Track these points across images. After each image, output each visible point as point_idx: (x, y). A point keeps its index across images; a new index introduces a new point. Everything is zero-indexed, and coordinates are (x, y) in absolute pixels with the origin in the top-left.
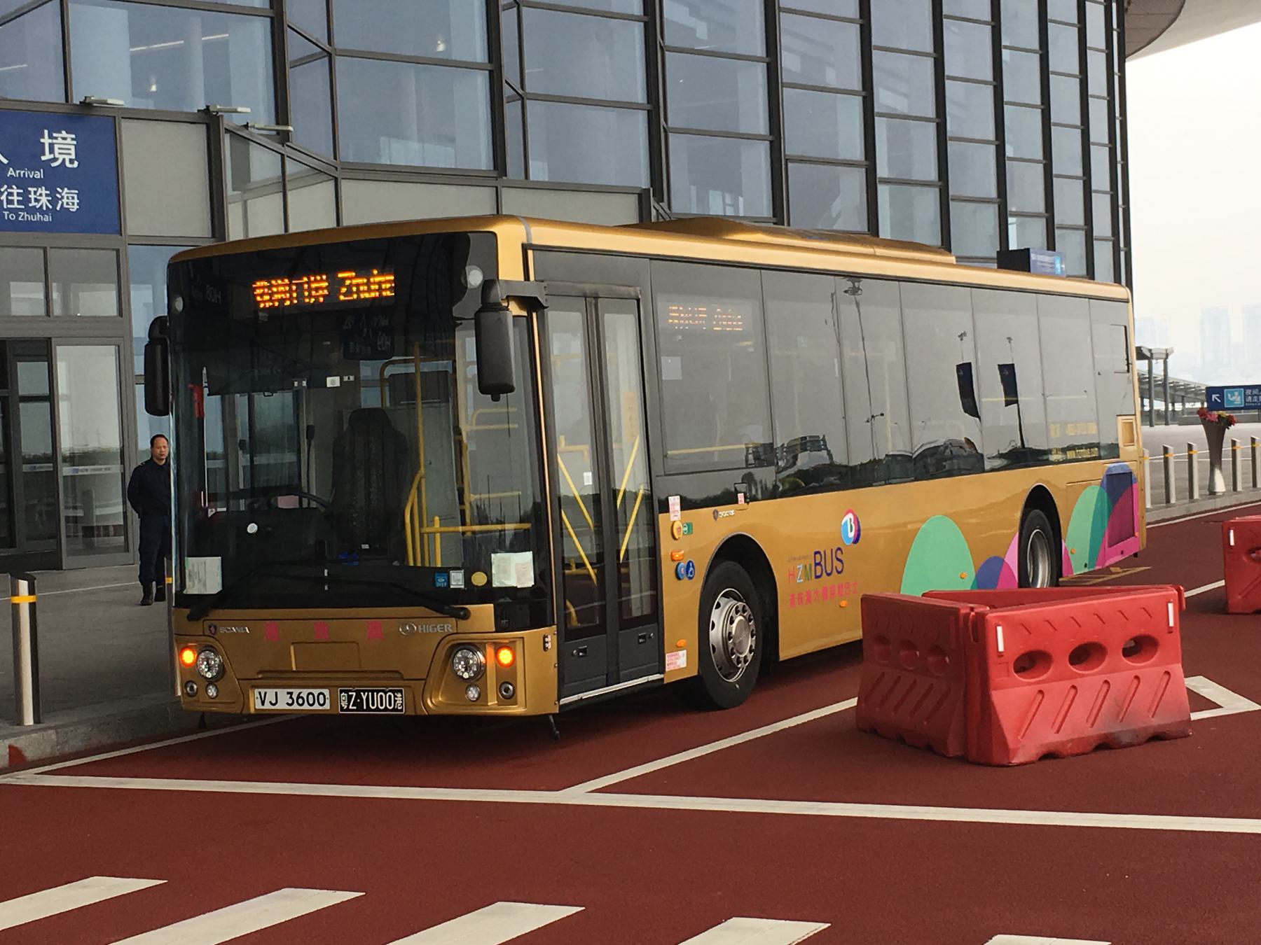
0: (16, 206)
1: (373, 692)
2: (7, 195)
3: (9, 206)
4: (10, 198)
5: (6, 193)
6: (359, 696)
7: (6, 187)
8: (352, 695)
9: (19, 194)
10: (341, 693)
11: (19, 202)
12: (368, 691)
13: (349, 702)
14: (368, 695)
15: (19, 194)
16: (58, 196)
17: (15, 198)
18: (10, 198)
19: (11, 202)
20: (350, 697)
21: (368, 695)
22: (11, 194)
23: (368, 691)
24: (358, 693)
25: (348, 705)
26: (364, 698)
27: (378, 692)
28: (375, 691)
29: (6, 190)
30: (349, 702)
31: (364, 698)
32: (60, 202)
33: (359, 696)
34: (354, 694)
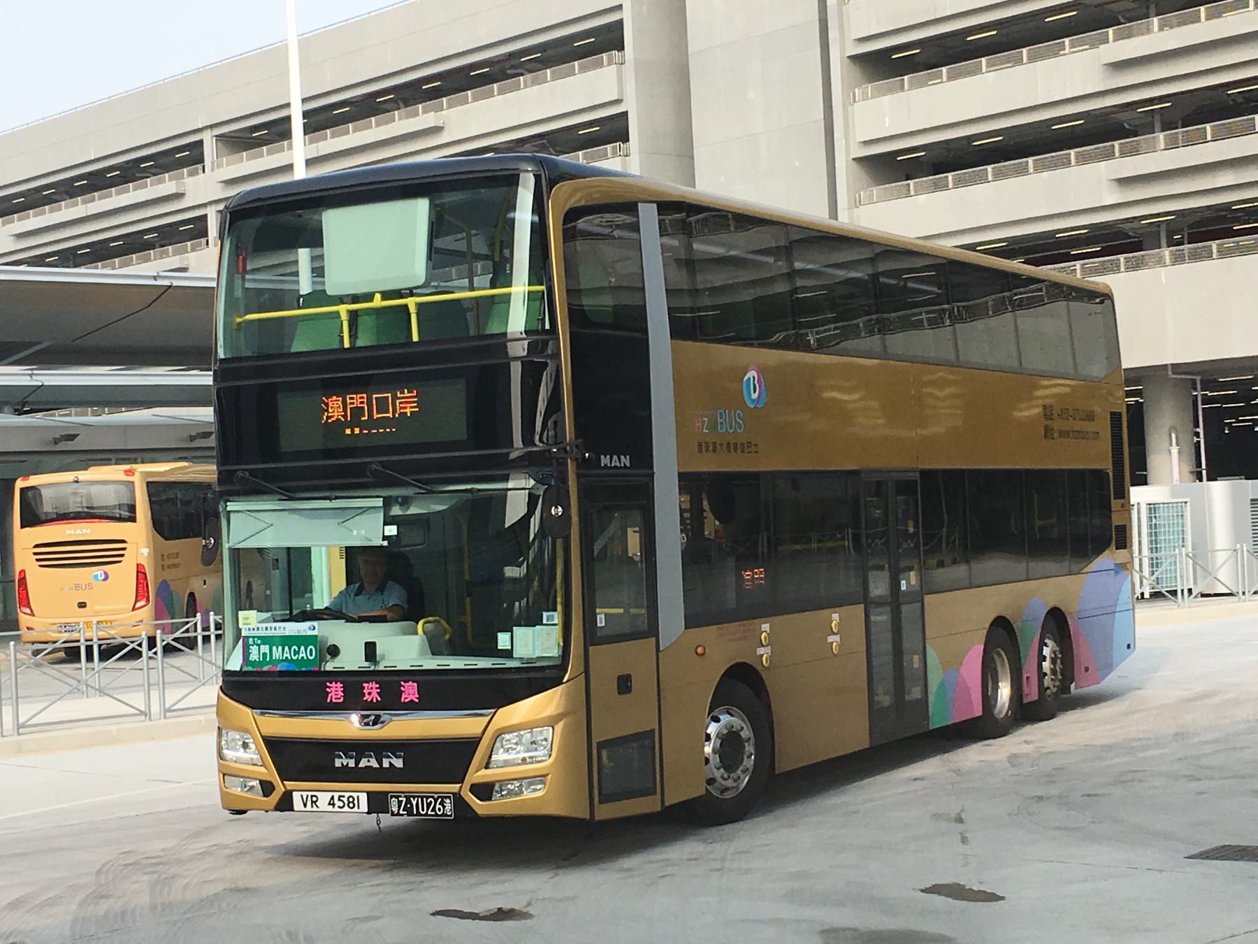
1: (422, 798)
6: (408, 801)
8: (402, 801)
10: (391, 798)
12: (418, 797)
13: (399, 807)
14: (418, 801)
20: (400, 803)
21: (418, 801)
23: (418, 797)
24: (408, 799)
25: (399, 810)
26: (414, 803)
27: (427, 798)
28: (425, 797)
30: (399, 807)
31: (414, 803)
33: (408, 801)
34: (404, 799)
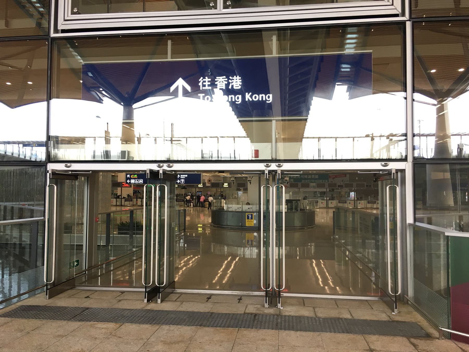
0: (207, 88)
2: (203, 83)
3: (204, 88)
4: (204, 83)
5: (202, 81)
7: (202, 78)
9: (209, 81)
11: (209, 85)
15: (209, 81)
16: (230, 81)
17: (207, 83)
18: (204, 83)
19: (204, 86)
22: (205, 82)
29: (202, 79)
32: (231, 85)
